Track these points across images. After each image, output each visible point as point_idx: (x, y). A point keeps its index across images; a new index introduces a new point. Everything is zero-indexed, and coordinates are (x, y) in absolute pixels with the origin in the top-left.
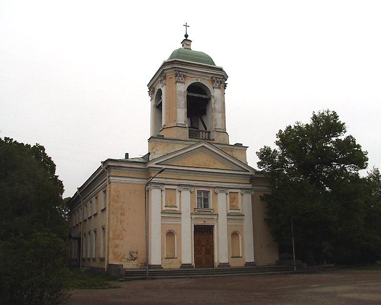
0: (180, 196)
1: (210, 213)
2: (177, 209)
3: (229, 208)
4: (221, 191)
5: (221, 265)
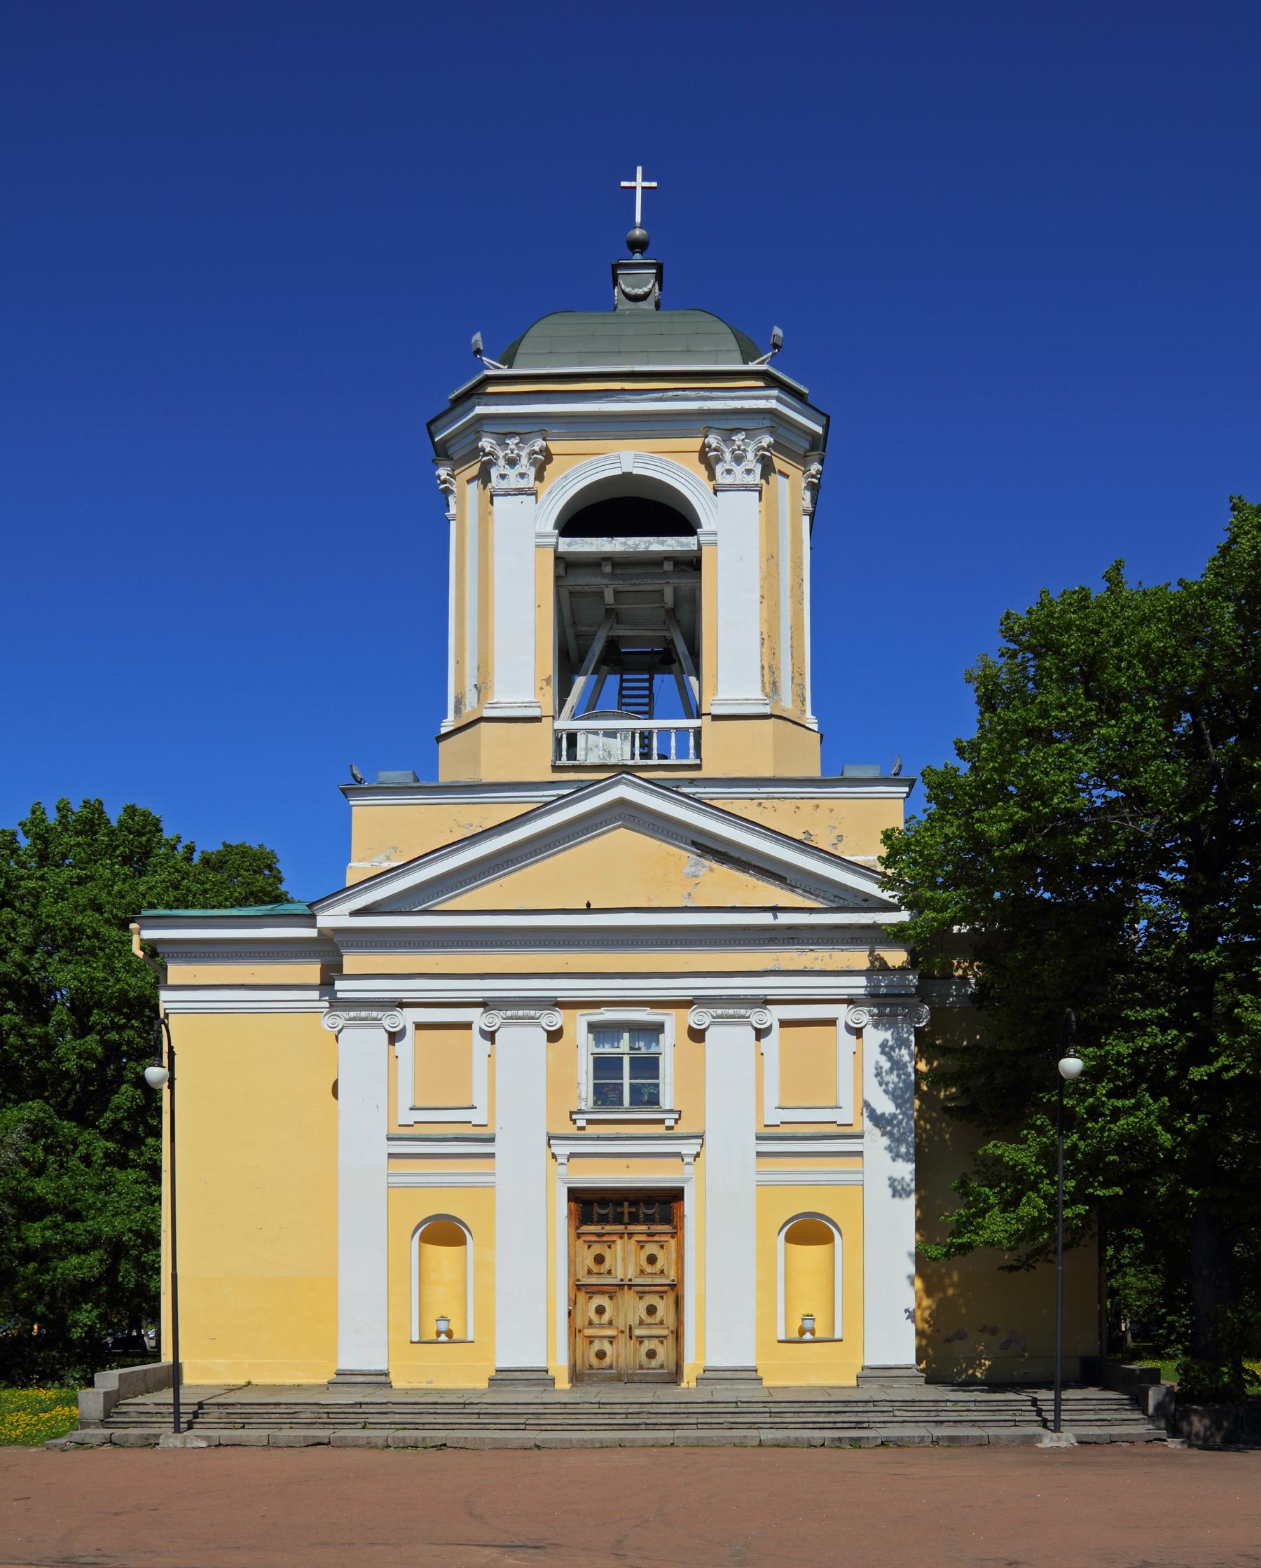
4: (719, 1021)
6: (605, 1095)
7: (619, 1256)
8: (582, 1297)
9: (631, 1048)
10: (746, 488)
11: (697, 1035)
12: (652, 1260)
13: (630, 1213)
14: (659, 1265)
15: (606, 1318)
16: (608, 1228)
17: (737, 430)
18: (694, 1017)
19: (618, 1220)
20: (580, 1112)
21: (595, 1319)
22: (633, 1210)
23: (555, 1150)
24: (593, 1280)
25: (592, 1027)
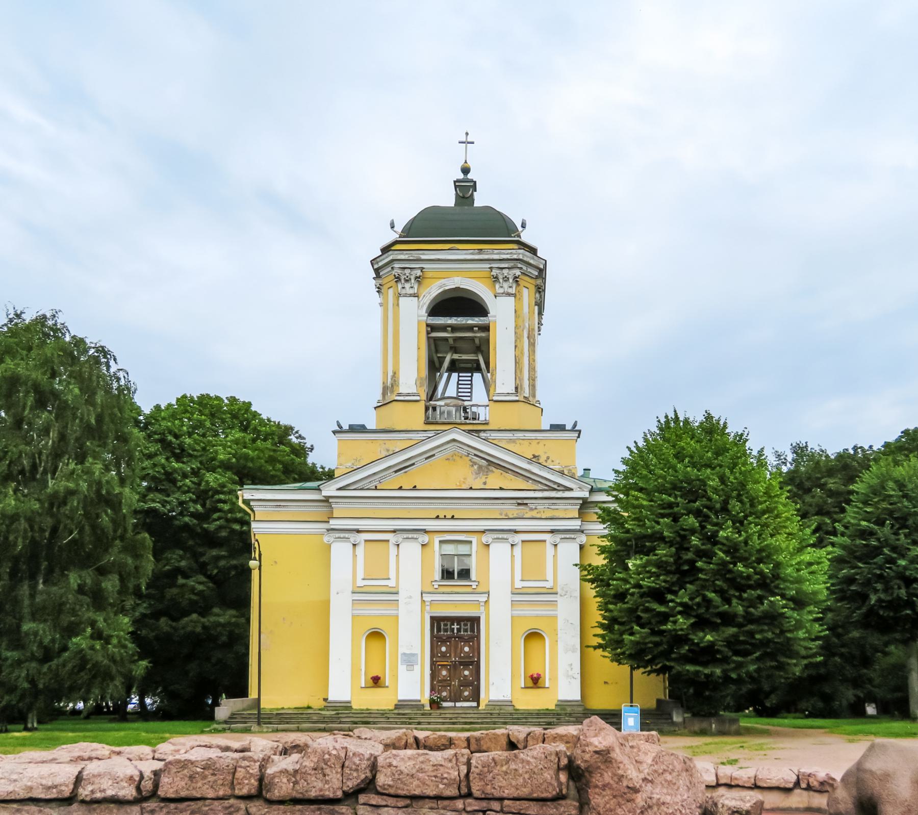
0: (397, 556)
1: (468, 590)
2: (392, 583)
3: (518, 576)
5: (493, 704)
6: (447, 574)
10: (509, 295)
18: (485, 539)
20: (436, 581)
25: (441, 542)
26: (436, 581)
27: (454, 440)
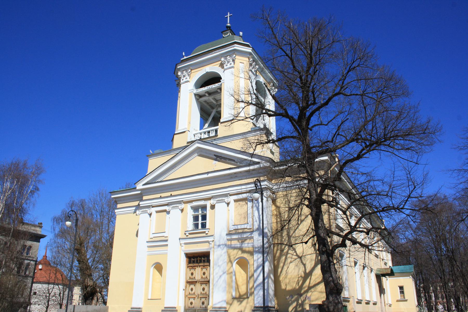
1: (204, 235)
4: (219, 202)
7: (197, 273)
8: (188, 285)
9: (202, 212)
11: (213, 207)
12: (204, 273)
13: (200, 260)
14: (206, 275)
15: (193, 291)
16: (195, 265)
17: (227, 56)
18: (212, 202)
19: (197, 262)
21: (191, 293)
22: (200, 259)
23: (181, 242)
24: (190, 280)
26: (187, 231)
27: (199, 148)
